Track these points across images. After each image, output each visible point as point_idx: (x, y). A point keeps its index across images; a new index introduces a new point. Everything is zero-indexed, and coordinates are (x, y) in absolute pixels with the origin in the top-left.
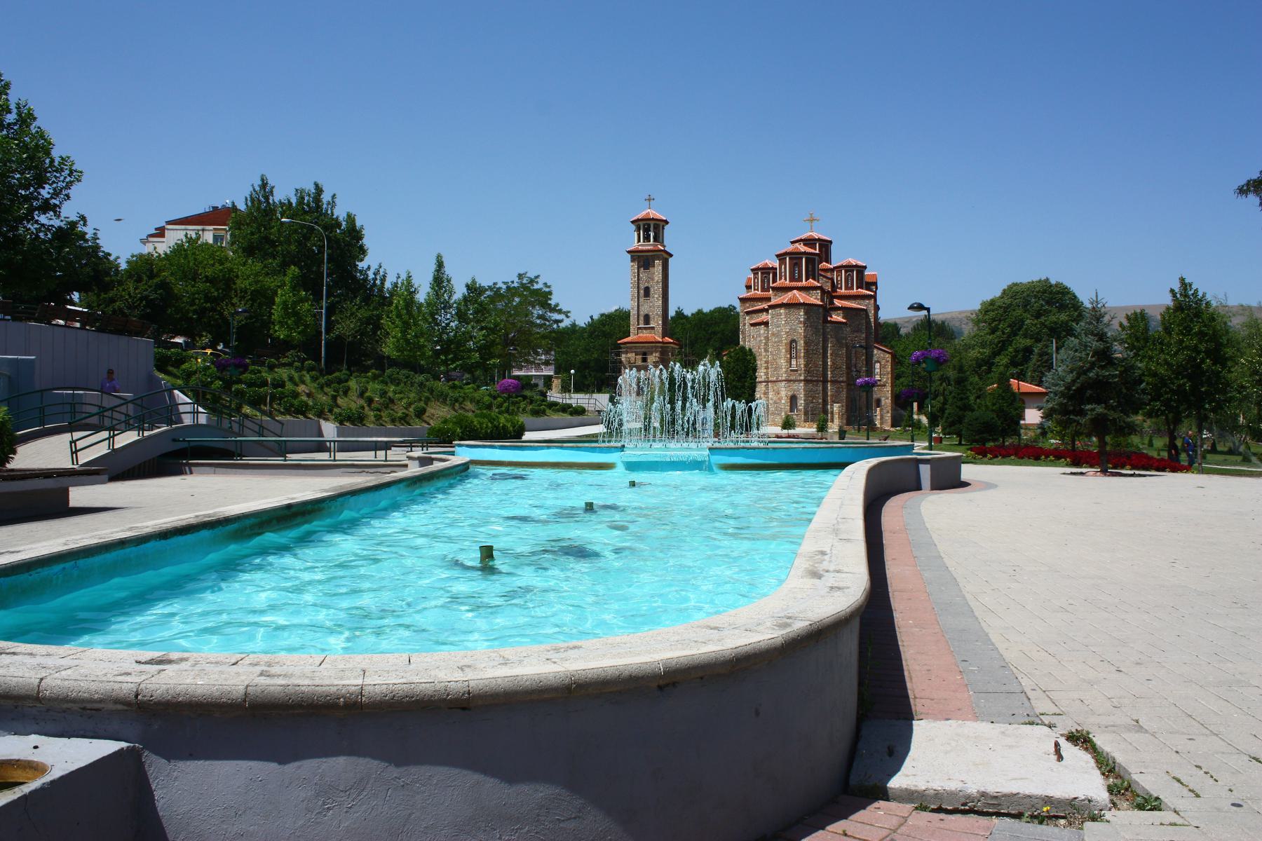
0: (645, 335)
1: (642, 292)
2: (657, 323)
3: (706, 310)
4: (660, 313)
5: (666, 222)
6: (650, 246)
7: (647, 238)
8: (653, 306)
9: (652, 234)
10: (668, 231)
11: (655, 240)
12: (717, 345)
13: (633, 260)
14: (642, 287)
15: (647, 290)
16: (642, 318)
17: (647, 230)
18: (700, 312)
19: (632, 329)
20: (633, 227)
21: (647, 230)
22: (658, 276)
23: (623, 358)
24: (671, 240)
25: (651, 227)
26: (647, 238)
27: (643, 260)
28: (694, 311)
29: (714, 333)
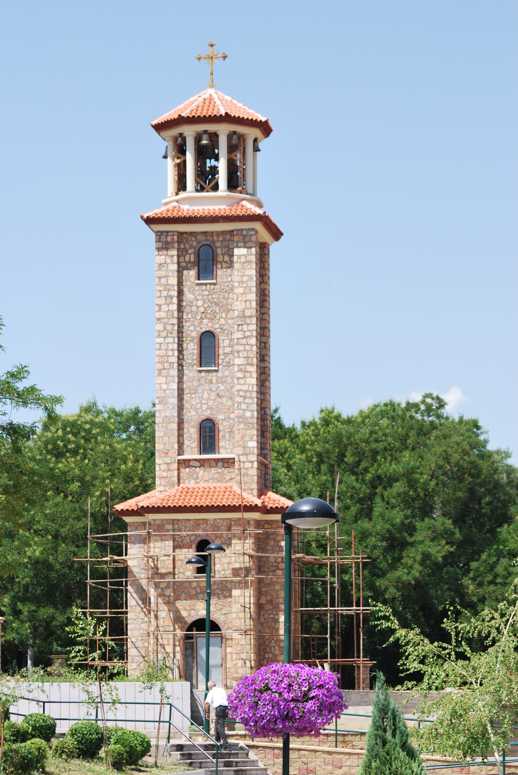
0: (205, 485)
1: (192, 349)
2: (240, 443)
3: (350, 407)
4: (251, 413)
5: (265, 128)
6: (218, 201)
7: (206, 179)
8: (227, 396)
9: (222, 165)
10: (267, 163)
11: (233, 184)
12: (398, 516)
13: (164, 246)
14: (192, 332)
15: (208, 341)
16: (192, 434)
17: (205, 152)
18: (329, 419)
19: (164, 465)
20: (161, 144)
21: (205, 152)
22: (245, 300)
23: (135, 557)
24: (276, 179)
25: (213, 146)
26: (206, 179)
27: (199, 249)
28: (313, 415)
29: (391, 480)
